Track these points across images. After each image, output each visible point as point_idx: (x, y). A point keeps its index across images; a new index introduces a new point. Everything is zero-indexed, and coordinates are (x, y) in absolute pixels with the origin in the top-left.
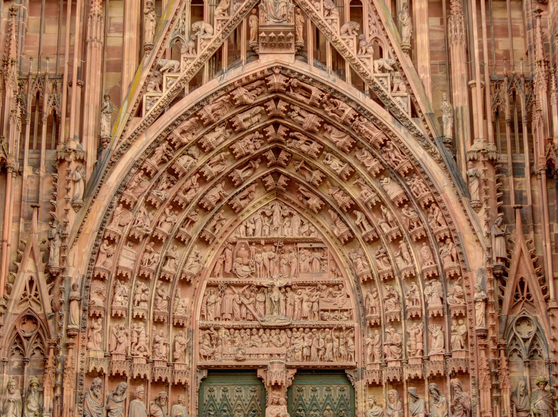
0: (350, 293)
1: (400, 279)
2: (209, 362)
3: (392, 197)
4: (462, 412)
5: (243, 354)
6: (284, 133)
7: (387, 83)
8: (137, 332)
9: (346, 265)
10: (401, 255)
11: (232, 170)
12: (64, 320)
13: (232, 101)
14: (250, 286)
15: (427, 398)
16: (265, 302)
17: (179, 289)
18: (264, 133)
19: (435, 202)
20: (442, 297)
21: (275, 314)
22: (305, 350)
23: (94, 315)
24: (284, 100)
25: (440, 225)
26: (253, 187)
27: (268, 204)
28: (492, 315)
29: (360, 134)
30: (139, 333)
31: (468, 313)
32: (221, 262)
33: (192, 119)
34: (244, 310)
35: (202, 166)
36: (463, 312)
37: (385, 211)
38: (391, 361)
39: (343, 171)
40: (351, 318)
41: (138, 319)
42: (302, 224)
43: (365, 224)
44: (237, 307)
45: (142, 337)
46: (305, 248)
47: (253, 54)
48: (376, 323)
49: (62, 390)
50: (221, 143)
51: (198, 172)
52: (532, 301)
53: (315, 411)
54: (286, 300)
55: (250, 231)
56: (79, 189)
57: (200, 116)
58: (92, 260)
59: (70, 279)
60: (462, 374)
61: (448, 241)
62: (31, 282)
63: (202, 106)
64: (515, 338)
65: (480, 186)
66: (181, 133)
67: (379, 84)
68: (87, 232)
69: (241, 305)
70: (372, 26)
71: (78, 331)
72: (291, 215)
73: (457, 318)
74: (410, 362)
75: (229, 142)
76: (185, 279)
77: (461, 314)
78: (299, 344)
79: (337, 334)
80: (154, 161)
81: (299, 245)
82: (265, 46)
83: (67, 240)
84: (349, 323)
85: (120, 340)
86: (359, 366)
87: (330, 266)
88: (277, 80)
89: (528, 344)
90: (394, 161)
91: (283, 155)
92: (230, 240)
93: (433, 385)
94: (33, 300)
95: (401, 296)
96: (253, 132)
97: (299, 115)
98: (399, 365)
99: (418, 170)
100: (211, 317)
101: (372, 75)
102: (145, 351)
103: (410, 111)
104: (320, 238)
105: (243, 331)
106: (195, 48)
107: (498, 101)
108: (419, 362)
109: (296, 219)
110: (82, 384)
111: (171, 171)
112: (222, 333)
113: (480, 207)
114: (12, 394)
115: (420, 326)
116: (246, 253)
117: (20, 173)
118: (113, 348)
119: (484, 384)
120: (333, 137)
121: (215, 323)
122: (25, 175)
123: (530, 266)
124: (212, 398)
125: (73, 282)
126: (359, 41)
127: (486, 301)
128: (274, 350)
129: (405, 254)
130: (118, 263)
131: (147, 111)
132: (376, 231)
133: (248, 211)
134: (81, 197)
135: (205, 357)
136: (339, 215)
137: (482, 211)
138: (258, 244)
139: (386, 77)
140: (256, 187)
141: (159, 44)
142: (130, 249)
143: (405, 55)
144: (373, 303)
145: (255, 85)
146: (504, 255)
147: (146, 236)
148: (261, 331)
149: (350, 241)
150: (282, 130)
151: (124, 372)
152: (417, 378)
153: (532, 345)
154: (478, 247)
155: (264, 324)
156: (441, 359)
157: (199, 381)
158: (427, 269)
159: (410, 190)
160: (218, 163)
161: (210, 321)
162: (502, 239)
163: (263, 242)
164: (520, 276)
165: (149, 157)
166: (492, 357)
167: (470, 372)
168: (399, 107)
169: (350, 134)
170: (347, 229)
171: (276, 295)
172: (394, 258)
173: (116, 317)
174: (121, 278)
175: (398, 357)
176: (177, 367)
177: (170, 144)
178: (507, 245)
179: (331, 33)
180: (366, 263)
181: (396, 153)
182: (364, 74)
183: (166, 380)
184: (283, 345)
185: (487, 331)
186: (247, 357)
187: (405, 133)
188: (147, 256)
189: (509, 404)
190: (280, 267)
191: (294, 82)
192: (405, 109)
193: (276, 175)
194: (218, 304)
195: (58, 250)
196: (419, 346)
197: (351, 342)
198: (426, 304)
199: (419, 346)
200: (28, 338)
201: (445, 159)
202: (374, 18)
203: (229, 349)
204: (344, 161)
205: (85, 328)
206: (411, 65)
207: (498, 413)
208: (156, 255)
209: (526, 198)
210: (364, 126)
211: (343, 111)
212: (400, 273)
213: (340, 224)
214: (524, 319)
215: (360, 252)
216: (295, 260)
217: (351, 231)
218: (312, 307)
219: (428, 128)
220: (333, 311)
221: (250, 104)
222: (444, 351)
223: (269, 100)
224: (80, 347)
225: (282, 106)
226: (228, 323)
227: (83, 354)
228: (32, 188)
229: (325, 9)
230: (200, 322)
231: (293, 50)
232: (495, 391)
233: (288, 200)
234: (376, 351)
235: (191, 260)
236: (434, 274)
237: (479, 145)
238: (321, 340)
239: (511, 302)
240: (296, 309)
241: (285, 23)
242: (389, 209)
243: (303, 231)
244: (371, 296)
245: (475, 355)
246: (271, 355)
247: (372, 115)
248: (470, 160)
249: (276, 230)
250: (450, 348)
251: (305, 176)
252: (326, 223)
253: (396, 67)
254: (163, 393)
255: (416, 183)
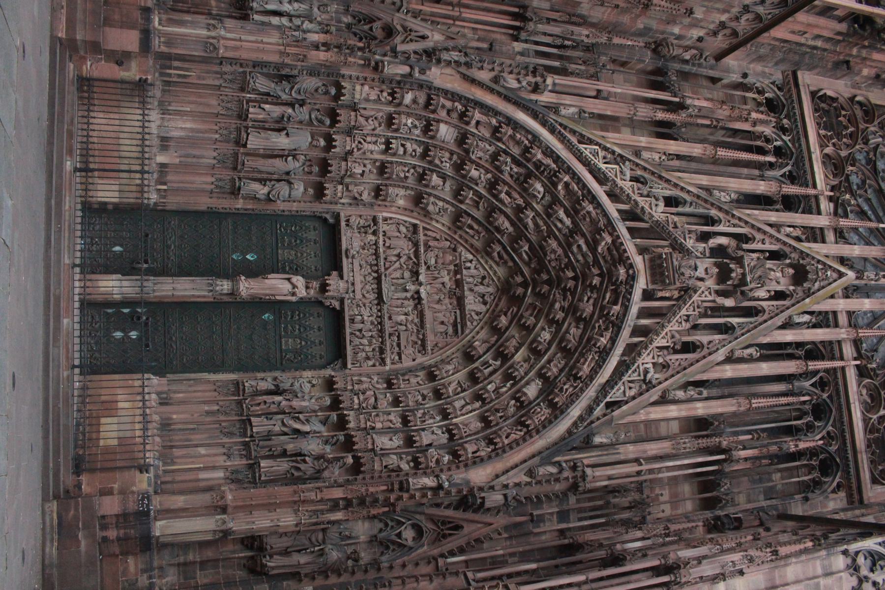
0: (417, 361)
1: (442, 404)
2: (343, 224)
3: (524, 390)
4: (317, 468)
5: (353, 257)
6: (569, 286)
7: (635, 377)
8: (377, 141)
9: (444, 356)
10: (467, 404)
11: (528, 240)
12: (391, 59)
13: (599, 231)
14: (418, 264)
15: (326, 434)
16: (403, 278)
17: (413, 193)
18: (567, 266)
19: (528, 432)
20: (435, 444)
21: (393, 288)
22: (360, 317)
23: (396, 93)
24: (602, 283)
25: (507, 437)
26: (510, 264)
27: (493, 281)
28: (424, 496)
29: (582, 355)
30: (375, 143)
31: (421, 471)
32: (438, 237)
33: (580, 192)
34: (394, 259)
35: (533, 209)
36: (422, 466)
37: (508, 385)
38: (359, 398)
39: (540, 343)
40: (392, 363)
41: (388, 143)
42: (478, 314)
43: (491, 369)
44: (396, 252)
45: (372, 147)
46: (456, 317)
47: (642, 251)
48: (393, 384)
49: (326, 51)
50: (556, 226)
51: (528, 205)
52: (440, 540)
53: (299, 330)
54: (406, 298)
55: (468, 264)
56: (514, 84)
57: (583, 200)
58: (446, 93)
59: (430, 69)
60: (356, 468)
61: (492, 447)
62: (423, 37)
63: (591, 203)
64: (400, 523)
65: (552, 474)
66: (566, 183)
67: (633, 368)
68: (473, 89)
69: (399, 256)
70: (678, 363)
71: (382, 71)
72: (485, 303)
73: (415, 460)
74: (361, 416)
75: (557, 233)
76: (423, 198)
77: (420, 463)
78: (366, 313)
79: (377, 349)
80: (539, 156)
81: (458, 312)
82: (651, 260)
83: (465, 68)
84: (388, 361)
85: (370, 121)
86: (347, 371)
87: (441, 342)
88: (622, 271)
89: (394, 538)
90: (562, 388)
91: (545, 288)
92: (458, 245)
93: (342, 438)
94: (406, 37)
95: (427, 406)
96: (567, 257)
97: (589, 299)
98: (356, 407)
99: (558, 412)
100: (386, 228)
101: (640, 361)
102: (359, 149)
103: (612, 400)
104: (467, 331)
105: (374, 257)
106: (641, 195)
107: (625, 491)
108: (363, 426)
109: (482, 308)
110: (328, 76)
111: (529, 175)
112: (371, 238)
113: (531, 477)
114: (319, 9)
115: (399, 425)
116: (447, 261)
117: (516, 39)
118: (362, 112)
119: (352, 490)
120: (573, 330)
121: (381, 230)
122: (515, 44)
123: (475, 535)
124: (308, 228)
125: (428, 72)
126: (667, 348)
127: (440, 487)
128: (358, 287)
129: (469, 407)
130: (442, 121)
131: (586, 149)
132: (485, 379)
133: (486, 262)
134: (506, 84)
135: (348, 221)
136: (493, 345)
137: (528, 480)
138: (456, 272)
139: (639, 375)
140: (510, 267)
141: (642, 163)
142: (454, 137)
143: (660, 393)
144: (413, 380)
145: (615, 252)
146: (488, 504)
147: (467, 152)
148: (375, 275)
149: (468, 357)
150: (571, 284)
151: (340, 121)
152: (348, 422)
153: (393, 542)
154: (491, 477)
155: (383, 277)
156: (370, 446)
157: (324, 215)
158: (459, 429)
159: (536, 405)
160: (536, 225)
161: (383, 227)
162: (503, 502)
163: (459, 276)
164: (465, 524)
165: (543, 153)
166: (381, 497)
167: (361, 476)
168: (615, 389)
169: (579, 345)
170: (481, 353)
171: (412, 287)
172: (464, 398)
173: (390, 121)
174: (427, 129)
175: (364, 405)
176: (340, 187)
177: (555, 172)
178: (495, 507)
179: (669, 322)
180: (451, 373)
181: (571, 389)
182: (639, 355)
183: (330, 172)
184: (364, 296)
185: (408, 491)
186: (350, 260)
187: (591, 397)
188: (447, 155)
189: (332, 518)
190: (437, 294)
191: (623, 289)
192: (615, 395)
193: (525, 285)
194: (398, 234)
195: (456, 59)
196: (379, 425)
197: (371, 363)
198: (423, 430)
199: (379, 425)
200: (371, 29)
201: (574, 437)
202: (684, 364)
203: (357, 244)
204: (550, 344)
205: (383, 82)
206: (652, 400)
207: (321, 507)
208: (448, 165)
209: (539, 527)
210: (591, 357)
211: (602, 336)
212: (450, 403)
213: (486, 345)
214: (419, 531)
215: (460, 368)
216: (444, 307)
217: (480, 357)
218: (401, 324)
219: (598, 419)
220: (399, 345)
221: (596, 249)
222: (378, 449)
223: (600, 268)
224: (365, 75)
225: (596, 281)
226: (381, 243)
227: (358, 78)
228: (504, 49)
229: (688, 316)
230: (381, 215)
231: (651, 287)
232: (344, 503)
233: (500, 299)
234: (365, 386)
235: (441, 204)
236: (454, 435)
237: (589, 471)
238: (370, 334)
239: (439, 516)
240: (399, 309)
241: (677, 276)
242: (510, 389)
243: (473, 314)
244: (419, 379)
245: (379, 480)
246: (353, 284)
247: (604, 363)
248: (575, 464)
249: (471, 290)
250: (383, 455)
251: (527, 310)
252: (483, 335)
253: (649, 385)
254: (316, 169)
255: (544, 412)
